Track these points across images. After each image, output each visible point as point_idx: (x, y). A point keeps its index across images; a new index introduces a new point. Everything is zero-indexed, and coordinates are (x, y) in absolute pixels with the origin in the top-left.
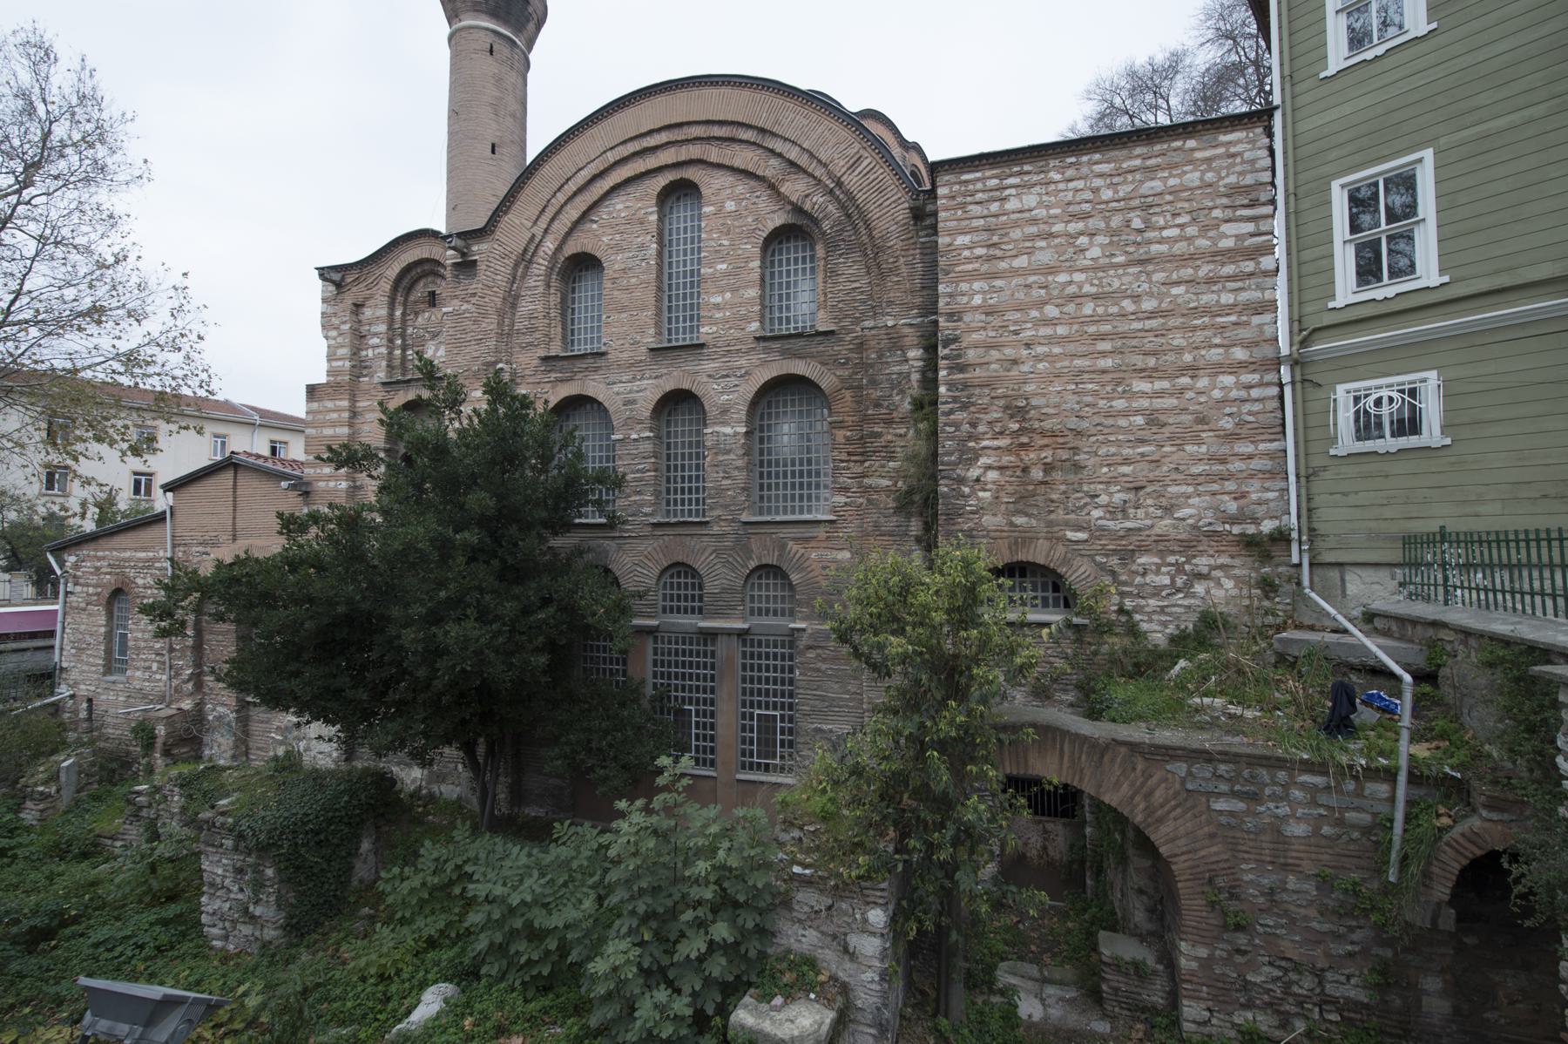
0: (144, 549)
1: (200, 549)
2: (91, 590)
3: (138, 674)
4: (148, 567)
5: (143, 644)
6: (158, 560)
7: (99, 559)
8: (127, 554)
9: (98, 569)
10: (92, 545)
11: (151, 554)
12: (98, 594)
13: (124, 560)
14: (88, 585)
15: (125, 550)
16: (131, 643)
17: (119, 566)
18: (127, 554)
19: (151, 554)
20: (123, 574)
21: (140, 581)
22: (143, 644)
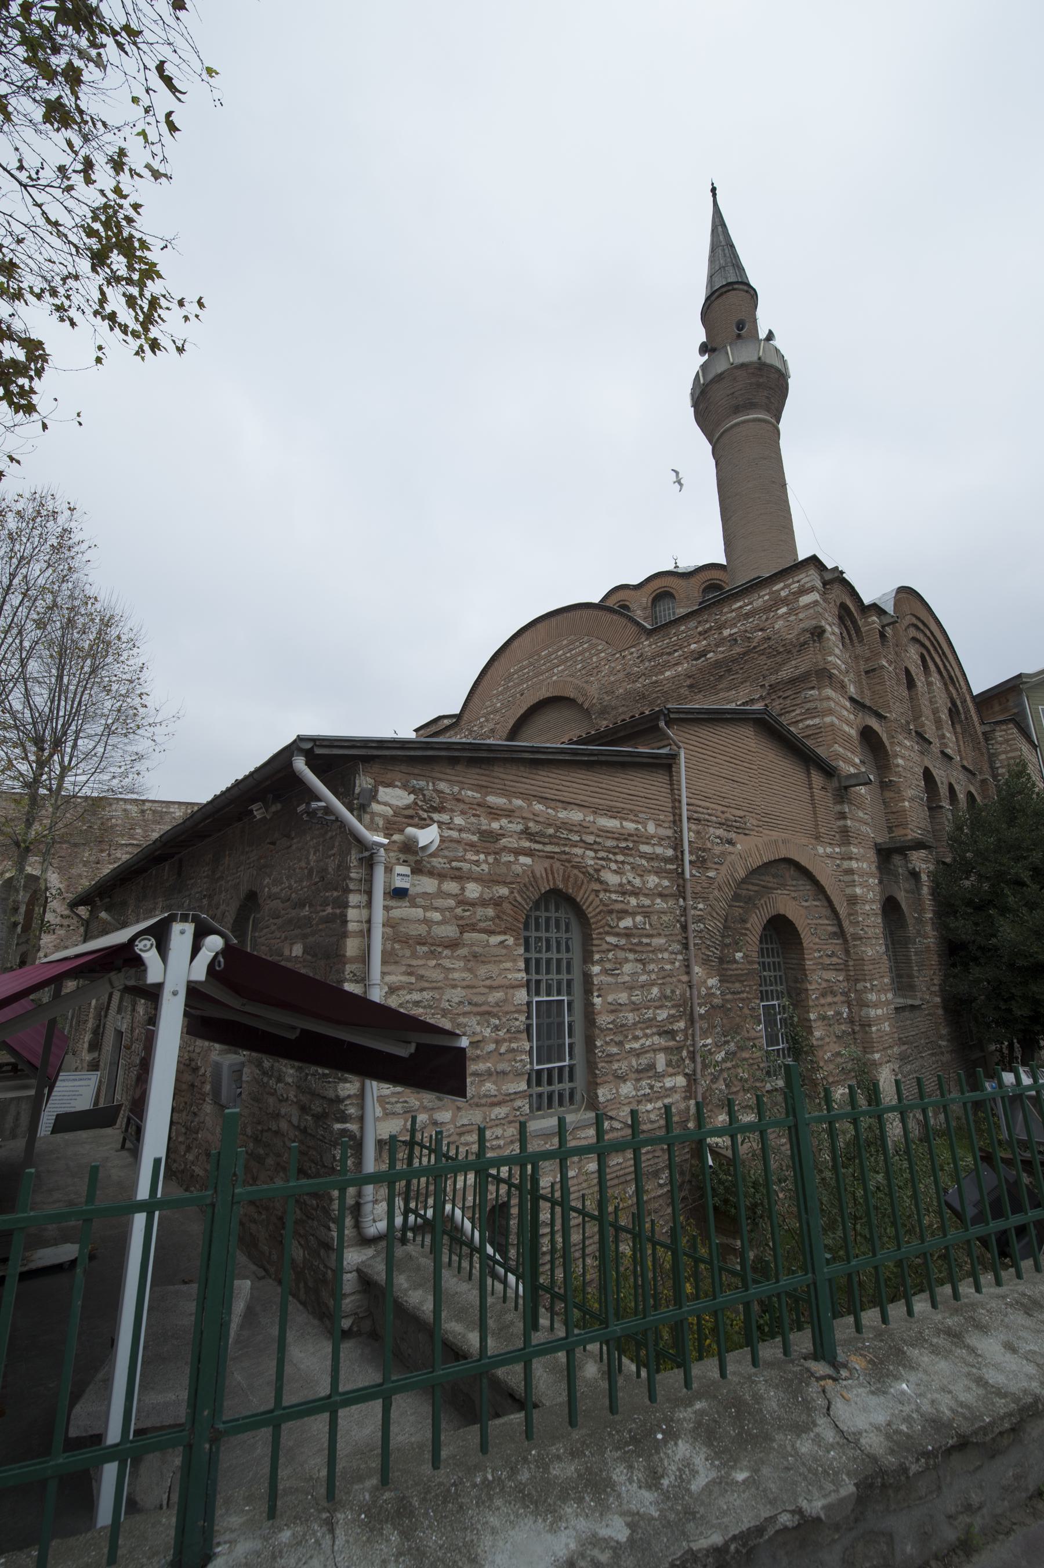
0: (612, 812)
1: (720, 832)
2: (473, 890)
3: (627, 1089)
4: (625, 851)
5: (631, 1017)
6: (648, 839)
7: (495, 813)
8: (576, 816)
9: (489, 838)
10: (474, 775)
11: (630, 826)
12: (497, 902)
13: (566, 826)
14: (459, 877)
15: (567, 804)
16: (604, 1020)
17: (553, 839)
18: (576, 816)
19: (630, 826)
20: (567, 860)
21: (612, 879)
22: (631, 1017)
